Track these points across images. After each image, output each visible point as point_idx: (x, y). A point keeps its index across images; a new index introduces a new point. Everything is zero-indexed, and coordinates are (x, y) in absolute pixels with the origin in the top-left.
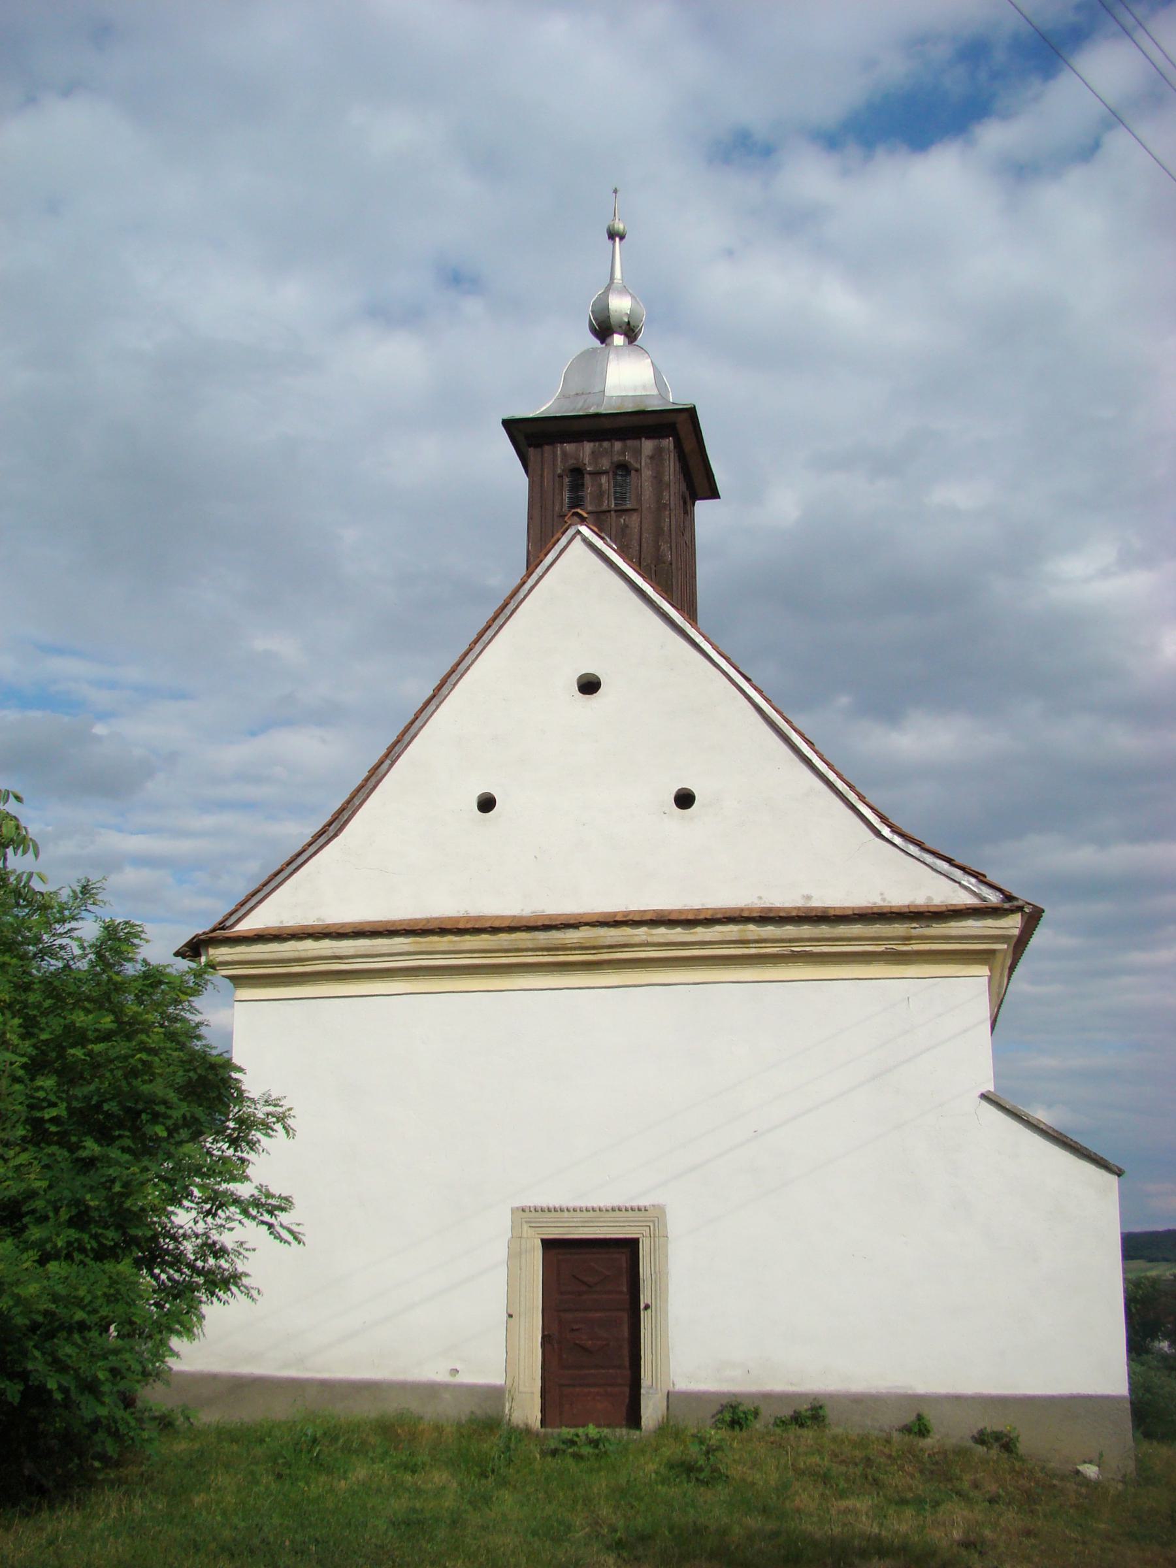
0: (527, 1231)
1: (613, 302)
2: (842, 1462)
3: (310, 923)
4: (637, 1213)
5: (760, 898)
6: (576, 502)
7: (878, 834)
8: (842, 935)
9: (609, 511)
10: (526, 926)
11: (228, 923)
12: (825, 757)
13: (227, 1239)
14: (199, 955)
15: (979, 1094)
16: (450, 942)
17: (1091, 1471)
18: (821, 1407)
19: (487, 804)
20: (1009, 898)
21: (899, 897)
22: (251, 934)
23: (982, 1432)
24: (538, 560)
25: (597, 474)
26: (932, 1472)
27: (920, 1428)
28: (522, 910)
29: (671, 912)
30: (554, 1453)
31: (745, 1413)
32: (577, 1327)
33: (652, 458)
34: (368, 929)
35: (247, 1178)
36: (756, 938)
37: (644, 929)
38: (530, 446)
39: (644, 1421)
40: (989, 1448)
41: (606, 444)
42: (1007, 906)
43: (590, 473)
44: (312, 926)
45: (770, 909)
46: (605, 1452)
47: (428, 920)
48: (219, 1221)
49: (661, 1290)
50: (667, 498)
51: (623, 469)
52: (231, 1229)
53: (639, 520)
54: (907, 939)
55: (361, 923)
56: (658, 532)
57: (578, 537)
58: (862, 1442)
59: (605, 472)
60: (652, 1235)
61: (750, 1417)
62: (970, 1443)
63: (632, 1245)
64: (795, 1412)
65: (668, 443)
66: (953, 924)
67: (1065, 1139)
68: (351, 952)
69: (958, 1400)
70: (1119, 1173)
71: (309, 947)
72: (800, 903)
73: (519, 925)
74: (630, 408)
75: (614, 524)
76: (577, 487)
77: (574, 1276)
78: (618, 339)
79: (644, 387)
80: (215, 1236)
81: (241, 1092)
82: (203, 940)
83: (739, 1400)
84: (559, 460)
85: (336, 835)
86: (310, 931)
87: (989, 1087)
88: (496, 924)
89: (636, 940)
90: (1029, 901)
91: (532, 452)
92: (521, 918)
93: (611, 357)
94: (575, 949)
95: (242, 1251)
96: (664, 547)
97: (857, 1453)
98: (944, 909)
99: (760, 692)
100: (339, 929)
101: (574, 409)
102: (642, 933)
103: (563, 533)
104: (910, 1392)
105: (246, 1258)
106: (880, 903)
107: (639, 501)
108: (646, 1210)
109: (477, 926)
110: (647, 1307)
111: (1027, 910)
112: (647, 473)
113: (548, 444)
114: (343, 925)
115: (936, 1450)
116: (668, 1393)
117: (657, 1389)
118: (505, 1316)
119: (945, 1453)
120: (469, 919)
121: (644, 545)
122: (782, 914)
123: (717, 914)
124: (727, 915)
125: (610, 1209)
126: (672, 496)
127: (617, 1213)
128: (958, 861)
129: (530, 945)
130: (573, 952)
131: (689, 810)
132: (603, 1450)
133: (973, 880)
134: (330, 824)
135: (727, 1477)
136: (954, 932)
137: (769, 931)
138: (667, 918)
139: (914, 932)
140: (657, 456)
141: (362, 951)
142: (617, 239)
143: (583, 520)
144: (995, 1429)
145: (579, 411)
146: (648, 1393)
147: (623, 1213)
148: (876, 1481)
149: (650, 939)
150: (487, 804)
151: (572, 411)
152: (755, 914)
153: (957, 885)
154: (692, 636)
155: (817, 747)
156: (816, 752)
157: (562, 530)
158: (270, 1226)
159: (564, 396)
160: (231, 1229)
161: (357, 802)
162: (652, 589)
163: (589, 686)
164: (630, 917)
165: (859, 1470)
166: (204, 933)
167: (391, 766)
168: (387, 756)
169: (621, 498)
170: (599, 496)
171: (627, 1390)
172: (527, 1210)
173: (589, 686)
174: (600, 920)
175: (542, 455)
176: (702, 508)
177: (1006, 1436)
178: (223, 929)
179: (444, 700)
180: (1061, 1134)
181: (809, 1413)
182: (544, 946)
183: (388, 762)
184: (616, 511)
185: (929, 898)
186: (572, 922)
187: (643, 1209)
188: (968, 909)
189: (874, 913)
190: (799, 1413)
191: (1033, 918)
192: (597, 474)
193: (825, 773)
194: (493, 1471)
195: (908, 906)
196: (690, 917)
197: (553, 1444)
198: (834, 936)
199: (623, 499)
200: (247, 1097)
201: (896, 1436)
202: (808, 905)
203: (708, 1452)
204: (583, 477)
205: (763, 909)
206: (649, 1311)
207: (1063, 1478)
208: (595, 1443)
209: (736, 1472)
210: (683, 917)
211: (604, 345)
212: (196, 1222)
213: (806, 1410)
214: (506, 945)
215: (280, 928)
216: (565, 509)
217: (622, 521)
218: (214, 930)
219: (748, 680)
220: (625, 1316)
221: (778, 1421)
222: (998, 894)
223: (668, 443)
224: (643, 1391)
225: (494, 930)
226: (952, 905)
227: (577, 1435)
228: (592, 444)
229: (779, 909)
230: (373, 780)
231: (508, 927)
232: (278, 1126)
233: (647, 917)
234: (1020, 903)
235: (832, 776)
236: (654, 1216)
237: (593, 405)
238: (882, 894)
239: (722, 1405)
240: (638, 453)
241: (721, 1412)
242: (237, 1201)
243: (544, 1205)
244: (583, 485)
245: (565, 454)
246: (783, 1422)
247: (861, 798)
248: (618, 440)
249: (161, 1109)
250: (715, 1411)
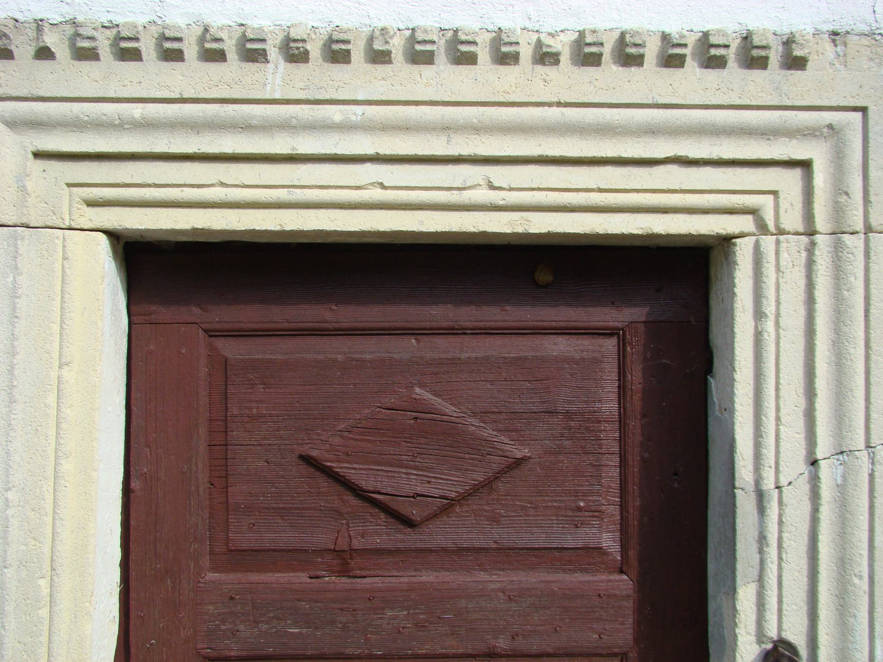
60: (821, 222)
77: (307, 460)
108: (795, 63)
125: (561, 45)
187: (775, 56)
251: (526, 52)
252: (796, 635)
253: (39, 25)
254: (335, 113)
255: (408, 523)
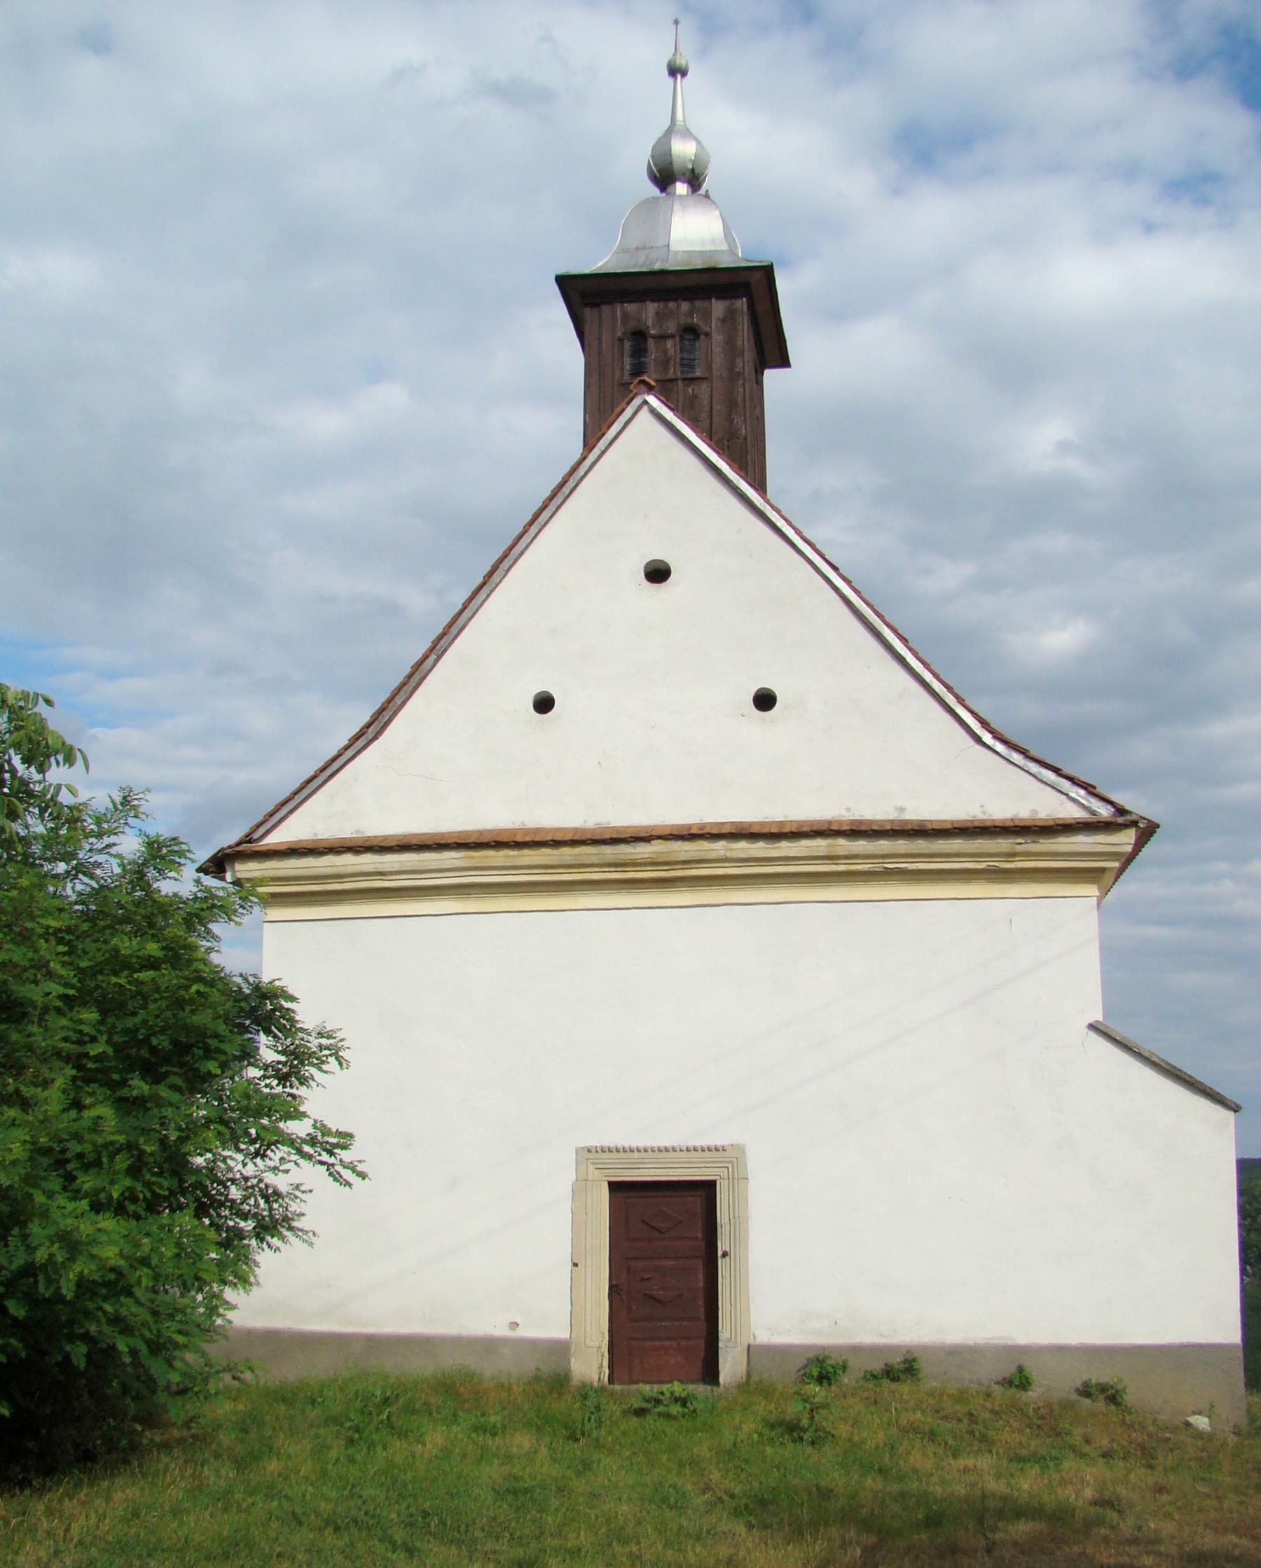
0: (593, 1173)
1: (676, 146)
2: (945, 1418)
3: (348, 835)
4: (714, 1154)
5: (848, 809)
6: (638, 370)
7: (978, 740)
8: (942, 851)
9: (677, 379)
10: (591, 840)
11: (256, 836)
12: (920, 655)
13: (281, 1182)
14: (224, 871)
15: (1087, 1024)
16: (507, 857)
17: (1201, 1422)
18: (914, 1360)
19: (544, 704)
20: (1121, 811)
21: (1001, 810)
22: (283, 848)
23: (1086, 1384)
24: (601, 433)
25: (662, 338)
26: (1039, 1427)
27: (1020, 1381)
28: (585, 822)
29: (751, 824)
30: (640, 1412)
31: (833, 1367)
32: (649, 1276)
33: (723, 321)
34: (414, 841)
35: (304, 1115)
36: (846, 853)
37: (722, 844)
38: (586, 305)
39: (721, 1380)
40: (1094, 1401)
41: (672, 305)
42: (1120, 820)
43: (654, 337)
44: (351, 839)
45: (860, 822)
46: (695, 1411)
47: (481, 833)
48: (271, 1164)
49: (740, 1237)
50: (741, 365)
51: (691, 332)
52: (287, 1171)
53: (709, 389)
54: (1012, 855)
55: (405, 836)
56: (732, 404)
57: (645, 408)
58: (962, 1396)
59: (672, 336)
60: (730, 1177)
61: (838, 1371)
62: (1074, 1397)
63: (707, 1189)
64: (886, 1365)
65: (742, 304)
66: (1062, 839)
67: (1179, 1073)
68: (396, 867)
69: (1061, 1350)
70: (1235, 1109)
71: (348, 861)
72: (893, 815)
73: (583, 838)
74: (699, 265)
75: (681, 394)
76: (639, 352)
77: (643, 1221)
78: (681, 188)
79: (713, 241)
80: (270, 1178)
81: (293, 1021)
82: (228, 855)
83: (826, 1354)
84: (619, 321)
85: (375, 738)
86: (350, 844)
87: (1097, 1016)
88: (558, 838)
89: (714, 855)
90: (1144, 816)
91: (588, 313)
92: (584, 830)
93: (675, 208)
94: (646, 864)
95: (297, 1193)
96: (738, 420)
97: (958, 1407)
98: (1052, 823)
99: (848, 582)
100: (382, 841)
101: (635, 266)
102: (720, 847)
103: (628, 403)
104: (1010, 1343)
105: (304, 1201)
106: (981, 816)
107: (709, 368)
108: (724, 1150)
109: (536, 839)
110: (725, 1254)
111: (1141, 825)
112: (718, 338)
113: (605, 303)
114: (386, 838)
115: (1040, 1404)
116: (749, 1346)
117: (736, 1343)
118: (570, 1264)
119: (1049, 1406)
120: (528, 831)
121: (716, 419)
122: (875, 828)
123: (803, 826)
124: (815, 828)
125: (684, 1149)
126: (747, 360)
127: (693, 1154)
128: (1067, 770)
129: (595, 860)
130: (644, 868)
131: (770, 712)
132: (692, 1409)
133: (1082, 792)
134: (368, 726)
135: (833, 1436)
136: (1062, 848)
137: (861, 846)
138: (748, 832)
139: (1019, 848)
140: (729, 319)
141: (409, 867)
142: (679, 76)
143: (650, 389)
144: (1101, 1381)
145: (641, 266)
146: (726, 1347)
147: (699, 1154)
148: (984, 1438)
149: (729, 854)
150: (544, 704)
151: (633, 268)
152: (845, 828)
153: (1064, 797)
154: (773, 520)
155: (911, 644)
156: (910, 649)
157: (628, 398)
158: (330, 1166)
159: (623, 250)
160: (287, 1171)
161: (398, 701)
162: (728, 467)
163: (657, 573)
164: (707, 830)
165: (964, 1426)
166: (230, 847)
167: (437, 661)
168: (432, 649)
169: (688, 364)
170: (665, 363)
171: (702, 1343)
172: (594, 1151)
173: (657, 573)
174: (675, 833)
175: (600, 315)
176: (771, 377)
177: (1112, 1387)
178: (250, 842)
179: (495, 588)
180: (1174, 1067)
181: (901, 1367)
182: (611, 862)
183: (433, 657)
184: (684, 380)
185: (1034, 811)
186: (643, 835)
188: (1078, 823)
189: (975, 828)
190: (891, 1367)
191: (1147, 831)
192: (662, 338)
193: (920, 673)
194: (583, 1434)
195: (1012, 820)
196: (774, 830)
197: (637, 1403)
198: (931, 851)
199: (692, 367)
200: (301, 1028)
201: (997, 1390)
202: (902, 818)
203: (812, 1410)
204: (646, 341)
205: (852, 822)
206: (728, 1258)
207: (1175, 1430)
208: (683, 1401)
209: (843, 1430)
210: (766, 830)
211: (664, 195)
212: (245, 1165)
213: (899, 1364)
214: (568, 860)
215: (315, 841)
216: (627, 378)
217: (690, 391)
218: (239, 844)
219: (835, 569)
220: (700, 1264)
221: (868, 1377)
222: (1109, 807)
223: (742, 304)
224: (721, 1345)
225: (556, 844)
226: (1059, 819)
227: (662, 1393)
228: (656, 305)
229: (871, 822)
230: (417, 677)
231: (571, 840)
232: (332, 1060)
233: (726, 830)
234: (1133, 817)
235: (928, 676)
236: (731, 1156)
237: (657, 260)
238: (982, 806)
239: (808, 1360)
240: (707, 315)
241: (806, 1366)
242: (291, 1142)
243: (612, 1145)
244: (646, 350)
245: (626, 316)
246: (875, 1377)
247: (960, 701)
248: (684, 300)
249: (213, 1043)
250: (801, 1365)
251: (678, 1149)
252: (728, 1250)
253: (596, 1147)
254: (646, 1161)
255: (662, 1233)
